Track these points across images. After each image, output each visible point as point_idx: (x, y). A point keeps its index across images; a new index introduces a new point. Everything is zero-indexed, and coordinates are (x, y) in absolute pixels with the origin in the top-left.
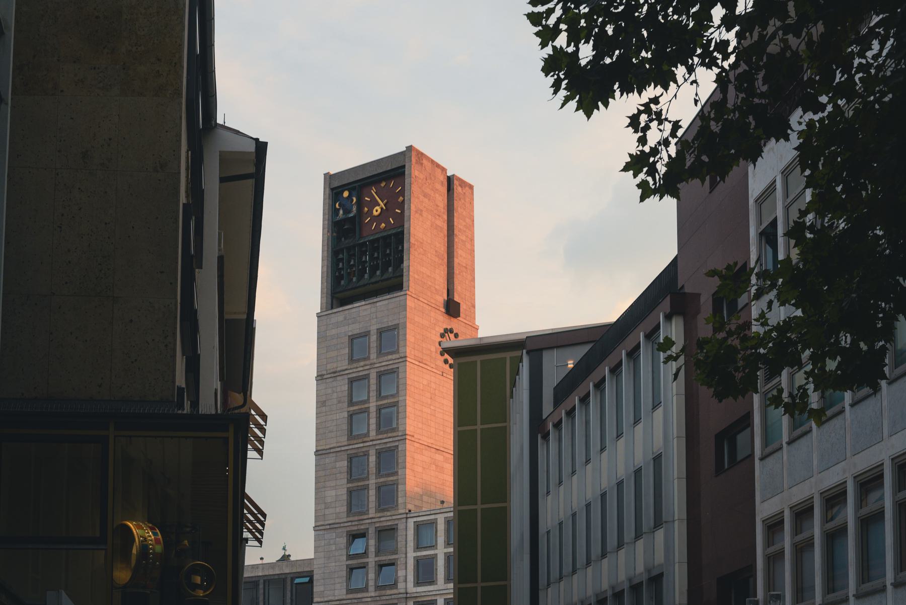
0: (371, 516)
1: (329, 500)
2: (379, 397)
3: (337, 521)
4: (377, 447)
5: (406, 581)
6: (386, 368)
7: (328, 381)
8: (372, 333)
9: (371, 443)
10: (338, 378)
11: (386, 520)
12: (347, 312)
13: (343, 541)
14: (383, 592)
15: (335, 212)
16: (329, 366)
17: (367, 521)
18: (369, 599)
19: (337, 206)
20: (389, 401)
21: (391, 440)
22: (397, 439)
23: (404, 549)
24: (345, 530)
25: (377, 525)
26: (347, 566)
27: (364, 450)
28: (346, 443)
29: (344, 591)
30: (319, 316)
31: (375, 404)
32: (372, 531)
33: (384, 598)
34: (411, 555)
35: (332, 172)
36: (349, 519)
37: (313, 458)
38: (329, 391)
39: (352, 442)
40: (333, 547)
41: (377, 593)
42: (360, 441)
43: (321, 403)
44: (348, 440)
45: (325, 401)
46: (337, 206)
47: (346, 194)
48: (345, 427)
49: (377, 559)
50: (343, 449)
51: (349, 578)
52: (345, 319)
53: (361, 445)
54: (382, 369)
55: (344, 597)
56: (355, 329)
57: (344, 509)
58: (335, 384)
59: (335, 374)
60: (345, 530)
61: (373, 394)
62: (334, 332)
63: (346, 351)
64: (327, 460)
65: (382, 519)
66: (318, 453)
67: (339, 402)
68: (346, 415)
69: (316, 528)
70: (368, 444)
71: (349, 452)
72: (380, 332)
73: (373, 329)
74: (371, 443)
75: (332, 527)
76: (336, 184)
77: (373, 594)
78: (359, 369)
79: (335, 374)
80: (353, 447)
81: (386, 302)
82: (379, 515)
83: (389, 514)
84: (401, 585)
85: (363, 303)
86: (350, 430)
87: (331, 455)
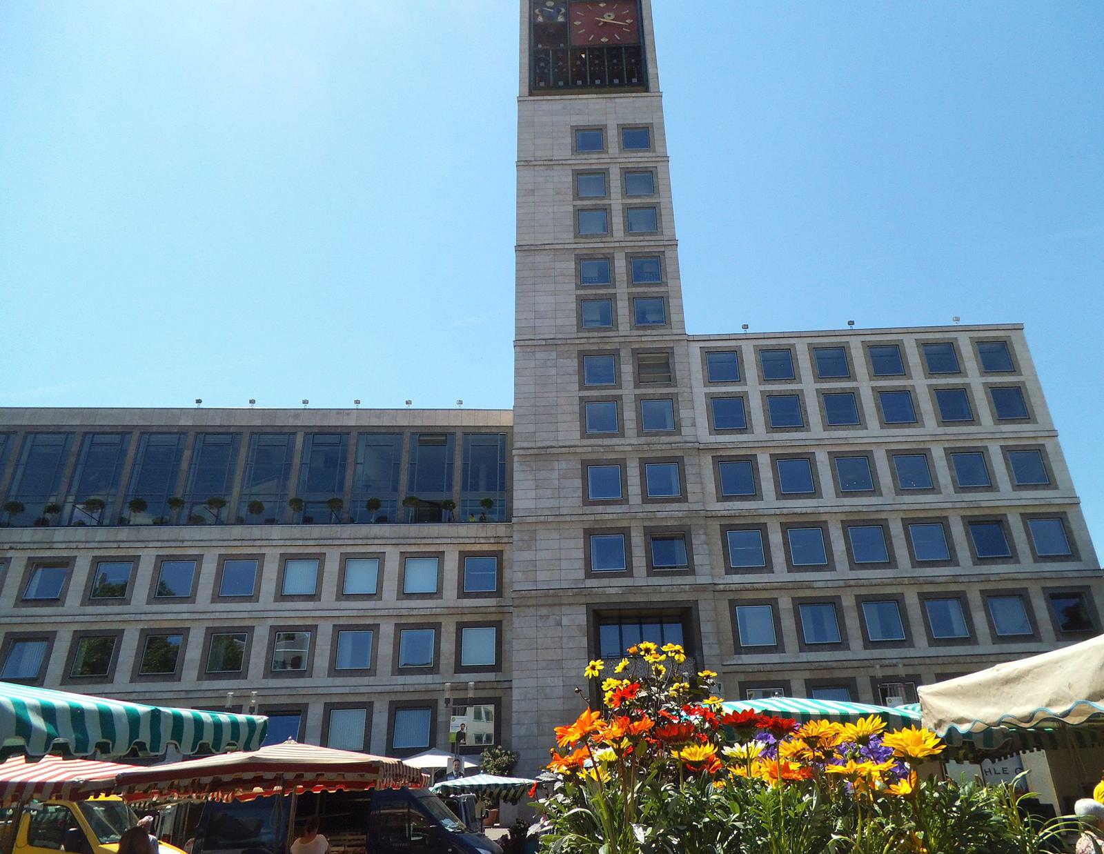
0: (621, 333)
5: (694, 425)
6: (636, 165)
7: (536, 168)
9: (617, 244)
10: (555, 168)
11: (651, 338)
12: (568, 102)
14: (655, 439)
16: (538, 154)
17: (617, 340)
18: (629, 448)
21: (652, 243)
22: (661, 243)
24: (576, 348)
27: (606, 251)
28: (572, 241)
29: (578, 435)
30: (520, 101)
36: (581, 335)
37: (511, 257)
39: (582, 240)
41: (643, 440)
42: (598, 240)
43: (525, 193)
44: (575, 237)
45: (533, 190)
46: (537, 11)
48: (570, 222)
50: (566, 246)
53: (602, 245)
54: (630, 166)
55: (578, 443)
56: (583, 121)
57: (574, 321)
59: (550, 164)
60: (576, 348)
64: (538, 259)
65: (643, 339)
66: (519, 248)
67: (558, 193)
68: (571, 209)
69: (518, 344)
70: (612, 245)
74: (617, 244)
75: (550, 344)
77: (634, 441)
78: (592, 160)
79: (550, 164)
80: (586, 246)
81: (631, 99)
83: (654, 332)
84: (686, 430)
85: (595, 96)
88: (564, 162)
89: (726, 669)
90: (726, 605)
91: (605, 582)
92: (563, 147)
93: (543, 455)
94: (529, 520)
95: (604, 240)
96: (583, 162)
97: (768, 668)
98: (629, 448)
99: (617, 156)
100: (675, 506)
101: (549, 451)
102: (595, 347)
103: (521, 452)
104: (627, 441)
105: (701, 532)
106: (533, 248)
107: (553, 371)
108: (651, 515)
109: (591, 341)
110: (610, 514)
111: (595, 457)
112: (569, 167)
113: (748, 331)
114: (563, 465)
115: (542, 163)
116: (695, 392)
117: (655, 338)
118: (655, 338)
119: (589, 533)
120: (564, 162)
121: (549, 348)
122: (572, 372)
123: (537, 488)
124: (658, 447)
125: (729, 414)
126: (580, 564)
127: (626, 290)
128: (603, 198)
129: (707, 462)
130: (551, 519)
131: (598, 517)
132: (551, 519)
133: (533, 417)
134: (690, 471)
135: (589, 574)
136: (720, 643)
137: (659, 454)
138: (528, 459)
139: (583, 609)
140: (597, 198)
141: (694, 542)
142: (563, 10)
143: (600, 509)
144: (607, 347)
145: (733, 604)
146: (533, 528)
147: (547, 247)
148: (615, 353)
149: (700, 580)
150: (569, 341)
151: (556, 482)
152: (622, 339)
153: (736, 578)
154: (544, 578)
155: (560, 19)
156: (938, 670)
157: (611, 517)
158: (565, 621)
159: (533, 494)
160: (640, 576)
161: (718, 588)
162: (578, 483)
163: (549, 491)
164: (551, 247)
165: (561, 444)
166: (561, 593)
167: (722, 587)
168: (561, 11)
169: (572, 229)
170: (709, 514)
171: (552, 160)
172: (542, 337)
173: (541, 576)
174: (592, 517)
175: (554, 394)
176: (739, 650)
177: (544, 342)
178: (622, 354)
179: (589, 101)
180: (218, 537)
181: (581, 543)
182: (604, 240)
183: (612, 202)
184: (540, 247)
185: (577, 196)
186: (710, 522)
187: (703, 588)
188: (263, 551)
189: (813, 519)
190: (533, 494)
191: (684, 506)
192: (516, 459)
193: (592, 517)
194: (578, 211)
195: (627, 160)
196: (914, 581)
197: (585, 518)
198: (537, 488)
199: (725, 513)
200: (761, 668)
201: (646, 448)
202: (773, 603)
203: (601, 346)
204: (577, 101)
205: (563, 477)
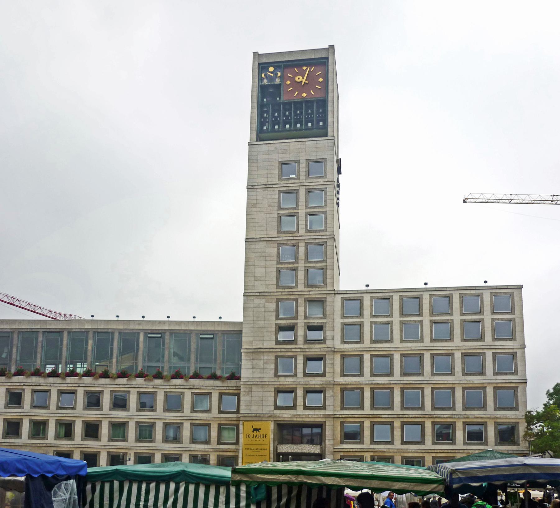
0: (299, 290)
1: (257, 275)
2: (307, 207)
3: (267, 291)
4: (306, 241)
5: (333, 339)
6: (315, 187)
7: (258, 190)
9: (301, 238)
10: (268, 189)
13: (273, 306)
15: (260, 79)
17: (297, 293)
19: (263, 76)
20: (318, 210)
23: (332, 316)
25: (307, 297)
26: (276, 324)
31: (304, 211)
32: (301, 301)
34: (338, 321)
38: (260, 197)
40: (263, 310)
41: (306, 346)
42: (290, 235)
43: (251, 205)
44: (278, 233)
46: (263, 76)
47: (271, 69)
48: (276, 224)
49: (306, 321)
50: (273, 239)
51: (277, 335)
52: (276, 149)
53: (292, 238)
54: (311, 187)
55: (274, 347)
56: (286, 157)
58: (265, 193)
59: (266, 186)
61: (302, 203)
62: (264, 157)
63: (277, 171)
64: (257, 246)
65: (311, 293)
67: (269, 206)
71: (278, 242)
72: (309, 161)
73: (303, 159)
75: (262, 295)
76: (264, 60)
77: (302, 346)
79: (266, 186)
80: (283, 239)
84: (329, 343)
85: (293, 140)
86: (279, 227)
87: (261, 243)
88: (274, 186)
89: (335, 450)
90: (339, 424)
91: (283, 412)
93: (257, 352)
95: (294, 235)
96: (285, 185)
97: (355, 450)
98: (299, 350)
99: (304, 181)
100: (319, 379)
101: (259, 350)
102: (285, 297)
103: (246, 350)
104: (298, 346)
105: (331, 391)
106: (254, 240)
107: (263, 310)
108: (307, 383)
109: (283, 294)
110: (287, 382)
111: (282, 354)
114: (266, 357)
115: (261, 187)
117: (317, 293)
118: (317, 293)
120: (274, 186)
121: (262, 297)
125: (351, 333)
126: (272, 403)
127: (304, 265)
128: (294, 209)
129: (338, 357)
130: (258, 383)
134: (328, 362)
136: (334, 439)
138: (249, 354)
139: (272, 423)
142: (279, 74)
143: (282, 379)
144: (292, 297)
146: (250, 386)
147: (262, 239)
149: (328, 412)
150: (271, 294)
151: (262, 366)
152: (300, 293)
154: (255, 409)
155: (278, 81)
157: (288, 383)
159: (251, 371)
160: (300, 410)
161: (336, 416)
162: (273, 366)
163: (259, 370)
164: (264, 239)
166: (262, 416)
167: (338, 416)
168: (278, 74)
169: (276, 228)
170: (336, 383)
171: (266, 185)
174: (278, 383)
175: (262, 322)
177: (258, 294)
178: (299, 301)
180: (109, 383)
182: (294, 235)
183: (300, 211)
184: (260, 240)
185: (280, 208)
186: (335, 386)
187: (329, 416)
188: (129, 389)
190: (251, 371)
191: (323, 379)
192: (243, 354)
194: (280, 216)
198: (253, 368)
199: (344, 383)
201: (307, 350)
203: (288, 297)
205: (265, 363)
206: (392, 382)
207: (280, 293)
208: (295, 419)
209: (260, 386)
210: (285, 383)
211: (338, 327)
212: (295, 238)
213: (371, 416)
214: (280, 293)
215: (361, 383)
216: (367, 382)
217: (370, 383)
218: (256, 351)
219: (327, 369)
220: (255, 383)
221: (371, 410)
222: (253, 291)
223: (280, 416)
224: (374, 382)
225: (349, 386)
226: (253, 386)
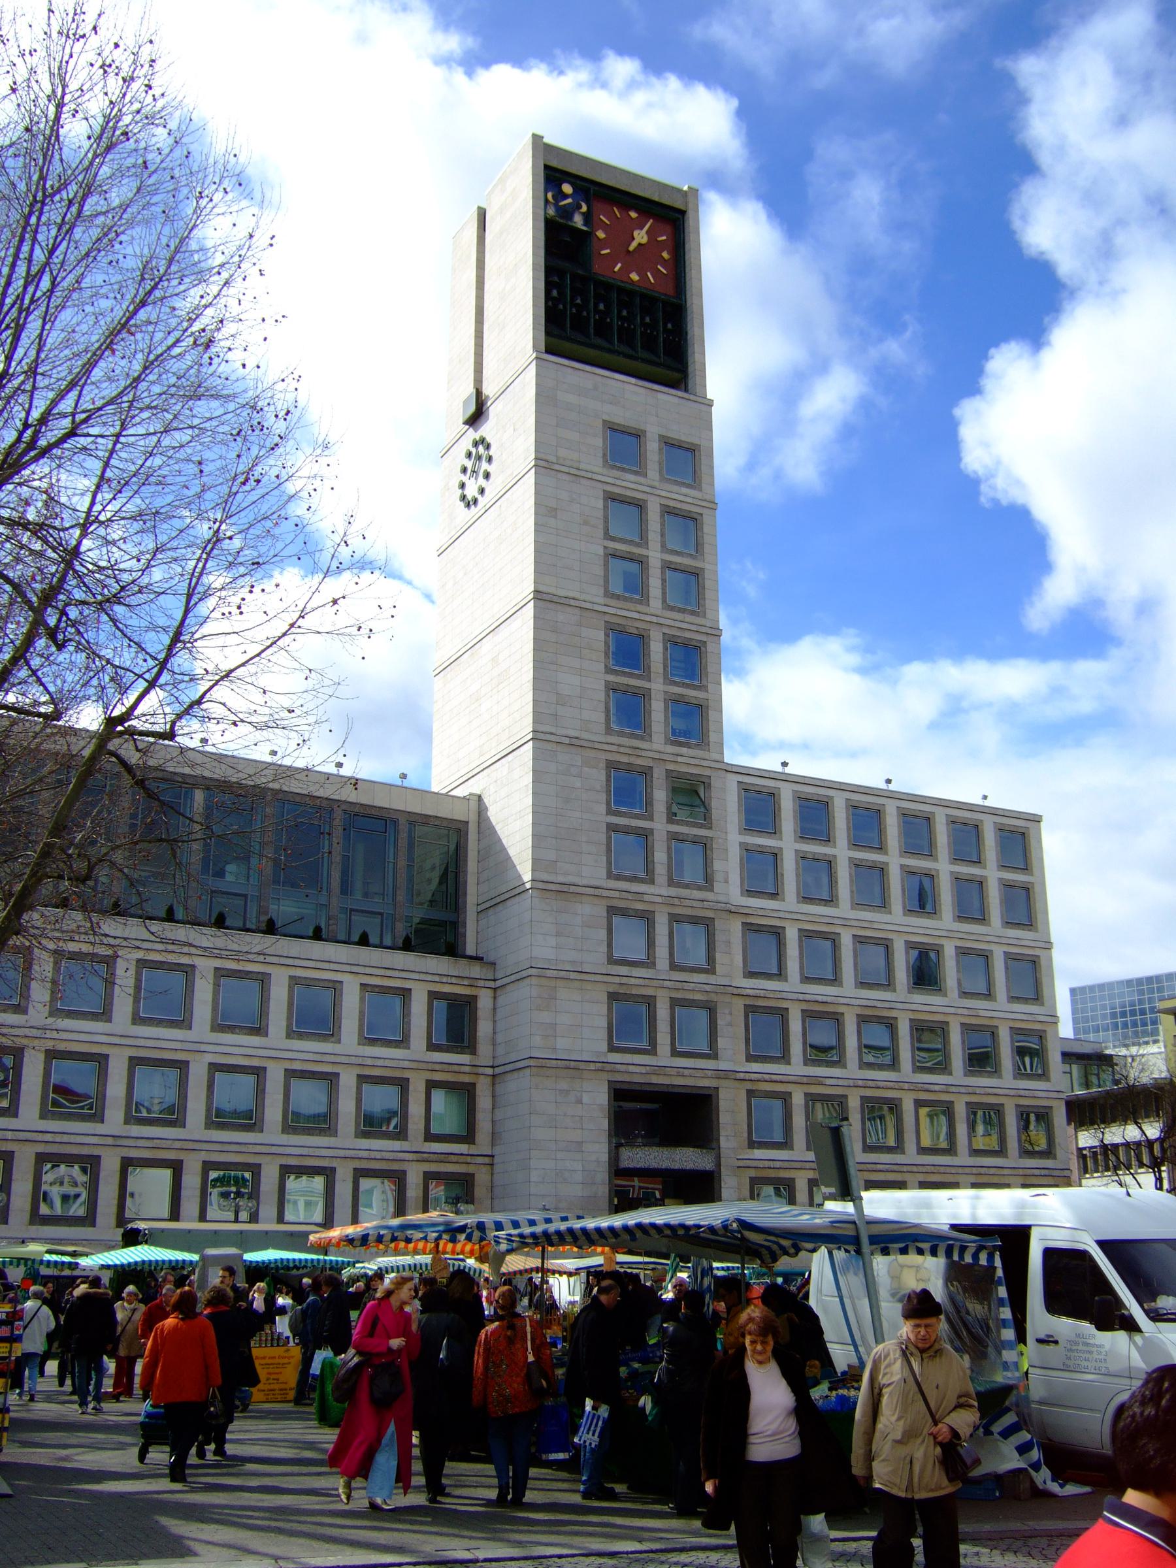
0: (655, 747)
4: (666, 631)
5: (727, 882)
6: (679, 505)
8: (648, 435)
9: (654, 619)
16: (562, 453)
18: (659, 900)
21: (694, 628)
24: (605, 756)
25: (671, 767)
33: (687, 903)
35: (546, 140)
41: (673, 891)
45: (556, 509)
53: (636, 616)
56: (620, 417)
65: (680, 759)
67: (586, 523)
68: (601, 552)
75: (575, 744)
77: (665, 891)
80: (620, 612)
81: (676, 400)
82: (671, 749)
84: (718, 887)
85: (633, 380)
87: (569, 609)
89: (741, 1163)
92: (590, 452)
94: (549, 973)
97: (778, 1164)
98: (659, 900)
99: (657, 484)
101: (572, 889)
102: (625, 759)
105: (727, 1011)
106: (555, 599)
108: (678, 985)
111: (622, 904)
112: (599, 485)
113: (787, 770)
116: (731, 835)
119: (613, 997)
121: (574, 749)
122: (598, 788)
123: (558, 934)
124: (687, 903)
125: (762, 872)
129: (736, 927)
131: (624, 980)
132: (573, 975)
133: (554, 841)
135: (612, 1049)
137: (689, 912)
138: (548, 894)
140: (631, 542)
141: (719, 1022)
143: (624, 970)
144: (639, 762)
145: (751, 1093)
146: (553, 983)
147: (572, 602)
148: (646, 773)
149: (723, 1065)
150: (597, 746)
152: (657, 756)
153: (756, 1067)
156: (921, 1178)
157: (637, 981)
158: (585, 1099)
165: (585, 882)
166: (582, 1065)
172: (564, 732)
173: (562, 1043)
176: (752, 1144)
179: (627, 387)
181: (604, 1009)
189: (830, 1009)
190: (552, 941)
191: (712, 979)
193: (617, 980)
195: (669, 495)
196: (915, 1087)
197: (610, 979)
200: (771, 1164)
201: (676, 902)
202: (786, 1098)
203: (632, 760)
204: (613, 382)
206: (842, 1000)
207: (614, 748)
208: (655, 1080)
209: (577, 984)
210: (633, 981)
211: (734, 853)
212: (643, 617)
213: (805, 1080)
214: (614, 748)
215: (784, 995)
216: (795, 996)
217: (801, 997)
218: (565, 888)
219: (718, 956)
220: (562, 974)
221: (805, 1064)
222: (553, 731)
223: (623, 1068)
224: (808, 997)
225: (761, 1003)
226: (560, 983)
